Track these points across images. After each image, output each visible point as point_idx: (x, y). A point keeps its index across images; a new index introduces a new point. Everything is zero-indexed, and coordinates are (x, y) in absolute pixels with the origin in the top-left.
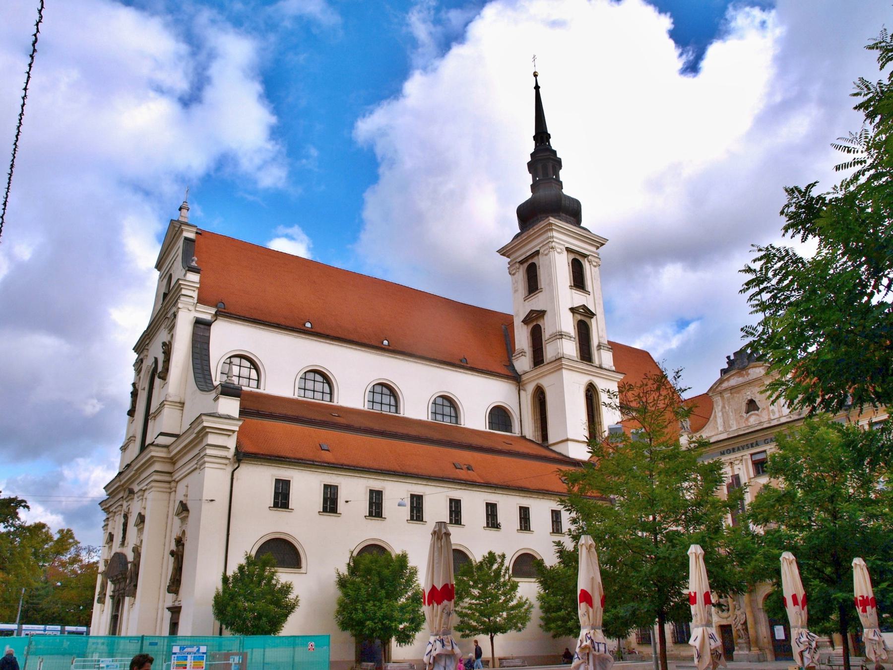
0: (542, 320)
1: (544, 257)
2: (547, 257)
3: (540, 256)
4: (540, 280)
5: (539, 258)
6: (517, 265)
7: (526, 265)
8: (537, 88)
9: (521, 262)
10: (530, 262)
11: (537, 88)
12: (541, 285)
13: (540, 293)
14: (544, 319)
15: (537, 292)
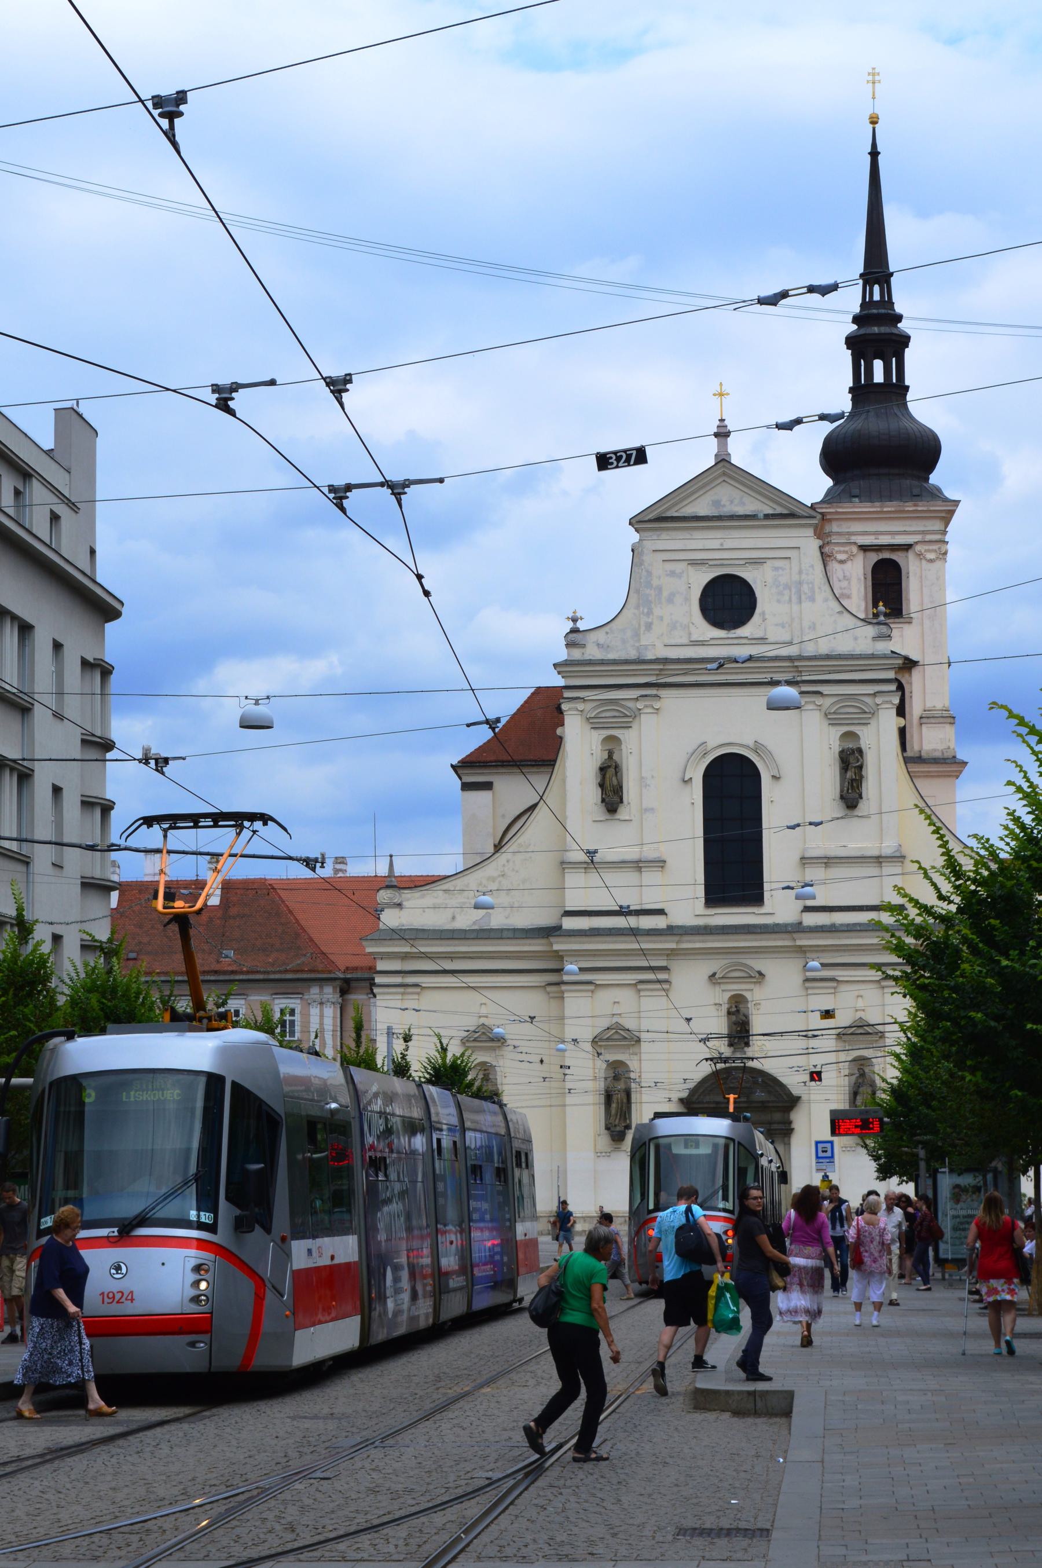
0: (907, 676)
1: (924, 562)
2: (930, 565)
3: (911, 555)
4: (908, 600)
5: (907, 557)
6: (855, 549)
7: (874, 557)
8: (874, 154)
9: (864, 548)
10: (886, 555)
11: (874, 154)
12: (908, 608)
13: (907, 625)
14: (911, 673)
15: (901, 620)
